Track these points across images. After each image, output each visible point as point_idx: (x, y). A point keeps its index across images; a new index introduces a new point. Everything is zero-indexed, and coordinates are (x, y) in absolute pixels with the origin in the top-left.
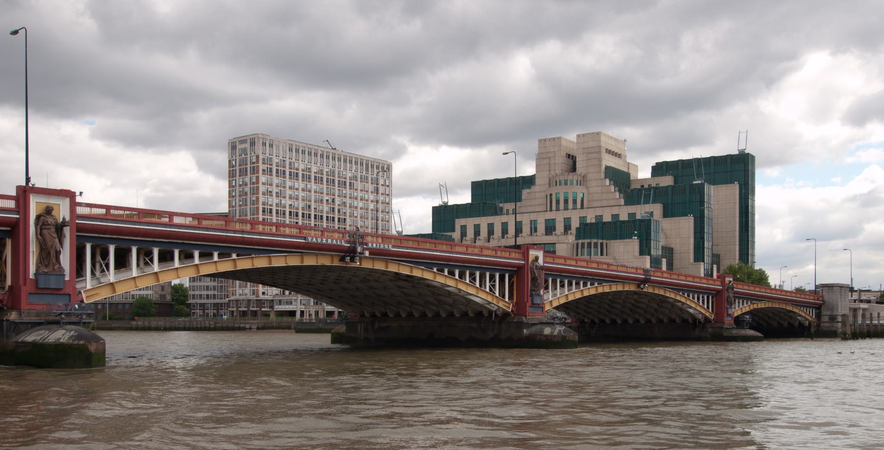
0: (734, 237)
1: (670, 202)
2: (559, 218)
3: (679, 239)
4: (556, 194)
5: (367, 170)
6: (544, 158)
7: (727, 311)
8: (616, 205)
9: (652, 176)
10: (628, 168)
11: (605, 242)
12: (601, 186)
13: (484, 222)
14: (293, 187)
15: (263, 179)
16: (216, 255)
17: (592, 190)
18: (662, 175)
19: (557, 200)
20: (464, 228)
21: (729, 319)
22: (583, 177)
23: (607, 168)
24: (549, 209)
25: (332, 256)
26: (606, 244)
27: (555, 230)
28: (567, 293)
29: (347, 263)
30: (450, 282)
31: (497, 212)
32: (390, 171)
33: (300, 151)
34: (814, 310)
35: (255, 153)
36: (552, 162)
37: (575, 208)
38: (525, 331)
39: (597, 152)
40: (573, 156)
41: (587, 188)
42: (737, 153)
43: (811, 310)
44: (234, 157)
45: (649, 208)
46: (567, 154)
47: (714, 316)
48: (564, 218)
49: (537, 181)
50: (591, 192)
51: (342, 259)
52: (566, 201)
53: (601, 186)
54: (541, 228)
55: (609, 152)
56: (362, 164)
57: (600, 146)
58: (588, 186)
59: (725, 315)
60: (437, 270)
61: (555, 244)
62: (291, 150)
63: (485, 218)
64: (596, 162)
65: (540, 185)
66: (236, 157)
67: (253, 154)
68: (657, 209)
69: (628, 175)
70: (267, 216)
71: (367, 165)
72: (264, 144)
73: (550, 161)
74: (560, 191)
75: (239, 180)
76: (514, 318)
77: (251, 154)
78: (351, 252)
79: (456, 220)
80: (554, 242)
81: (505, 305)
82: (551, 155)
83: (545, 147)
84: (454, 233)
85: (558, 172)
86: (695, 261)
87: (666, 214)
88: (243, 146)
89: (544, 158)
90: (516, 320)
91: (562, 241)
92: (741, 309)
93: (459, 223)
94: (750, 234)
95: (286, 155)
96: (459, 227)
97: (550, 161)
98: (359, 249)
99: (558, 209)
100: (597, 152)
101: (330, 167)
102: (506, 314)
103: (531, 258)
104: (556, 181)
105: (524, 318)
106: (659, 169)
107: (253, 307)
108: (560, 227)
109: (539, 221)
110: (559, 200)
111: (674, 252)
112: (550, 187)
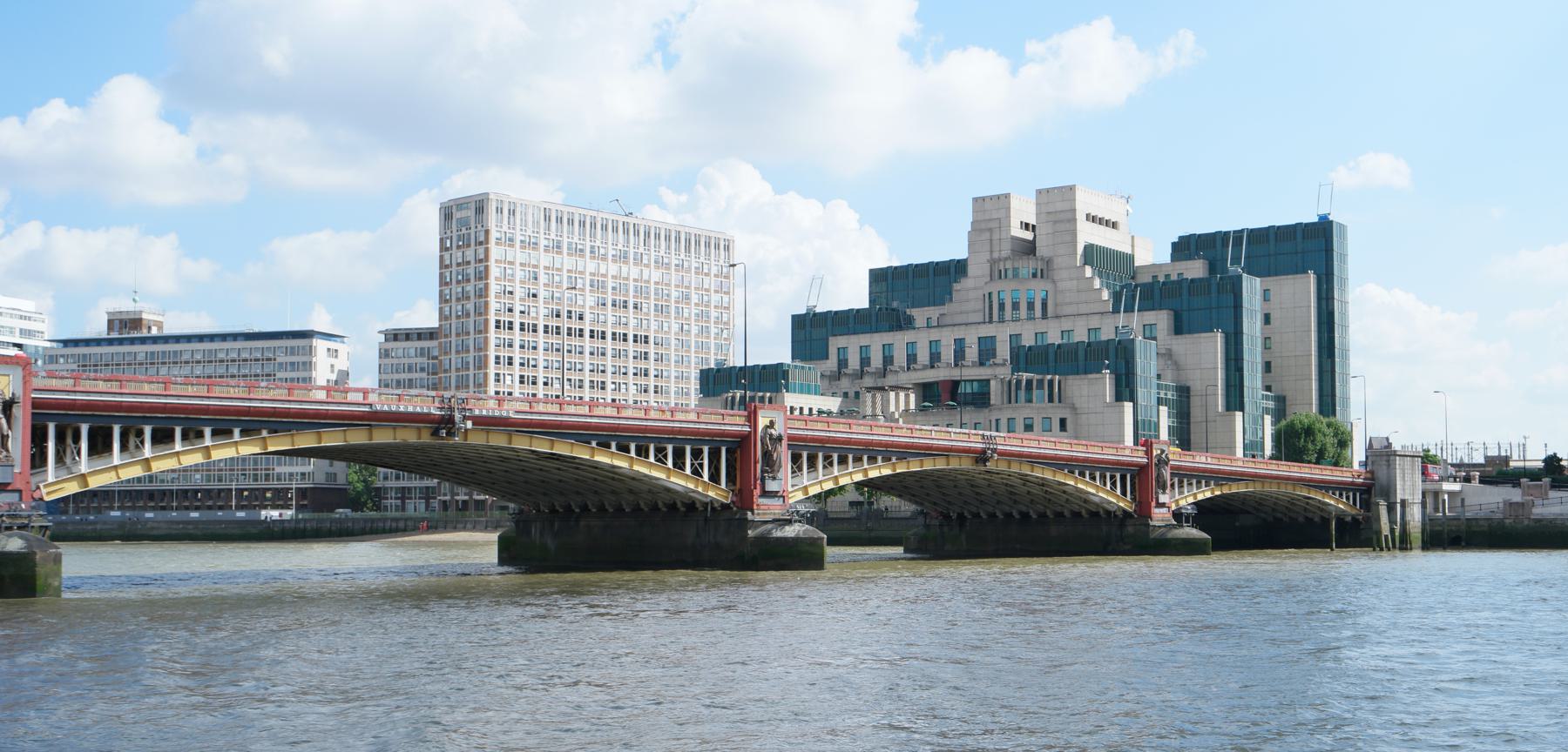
0: (1310, 365)
1: (1184, 308)
2: (1002, 336)
3: (1199, 371)
4: (999, 292)
5: (688, 249)
7: (1157, 499)
8: (1095, 311)
9: (1172, 261)
10: (1133, 246)
13: (876, 342)
16: (237, 432)
17: (1061, 285)
18: (1190, 258)
19: (1000, 304)
20: (842, 351)
21: (1164, 510)
23: (1089, 248)
24: (987, 320)
25: (419, 428)
26: (1059, 382)
27: (994, 356)
28: (836, 474)
29: (442, 438)
30: (621, 463)
31: (903, 323)
32: (731, 251)
33: (565, 220)
34: (1358, 495)
35: (482, 226)
36: (996, 236)
37: (1031, 318)
38: (749, 532)
42: (1316, 220)
43: (1351, 494)
45: (1150, 317)
46: (1021, 222)
47: (1136, 506)
48: (979, 338)
49: (971, 270)
51: (435, 433)
52: (1016, 306)
54: (972, 353)
55: (1093, 219)
56: (678, 239)
58: (1055, 278)
59: (1153, 504)
60: (597, 444)
62: (547, 218)
65: (975, 278)
66: (452, 232)
67: (479, 226)
68: (1161, 319)
69: (1131, 258)
70: (504, 334)
72: (499, 210)
73: (991, 236)
74: (1006, 290)
76: (736, 514)
77: (476, 227)
78: (445, 423)
81: (718, 494)
82: (993, 225)
83: (985, 211)
84: (828, 361)
87: (1178, 329)
88: (462, 214)
90: (737, 517)
92: (1195, 495)
93: (836, 343)
94: (1337, 360)
95: (539, 227)
96: (836, 351)
97: (991, 236)
98: (457, 416)
99: (1002, 320)
101: (620, 247)
102: (725, 507)
103: (762, 422)
104: (1000, 271)
105: (749, 513)
106: (1185, 247)
109: (968, 341)
110: (1004, 304)
111: (1192, 394)
112: (991, 279)
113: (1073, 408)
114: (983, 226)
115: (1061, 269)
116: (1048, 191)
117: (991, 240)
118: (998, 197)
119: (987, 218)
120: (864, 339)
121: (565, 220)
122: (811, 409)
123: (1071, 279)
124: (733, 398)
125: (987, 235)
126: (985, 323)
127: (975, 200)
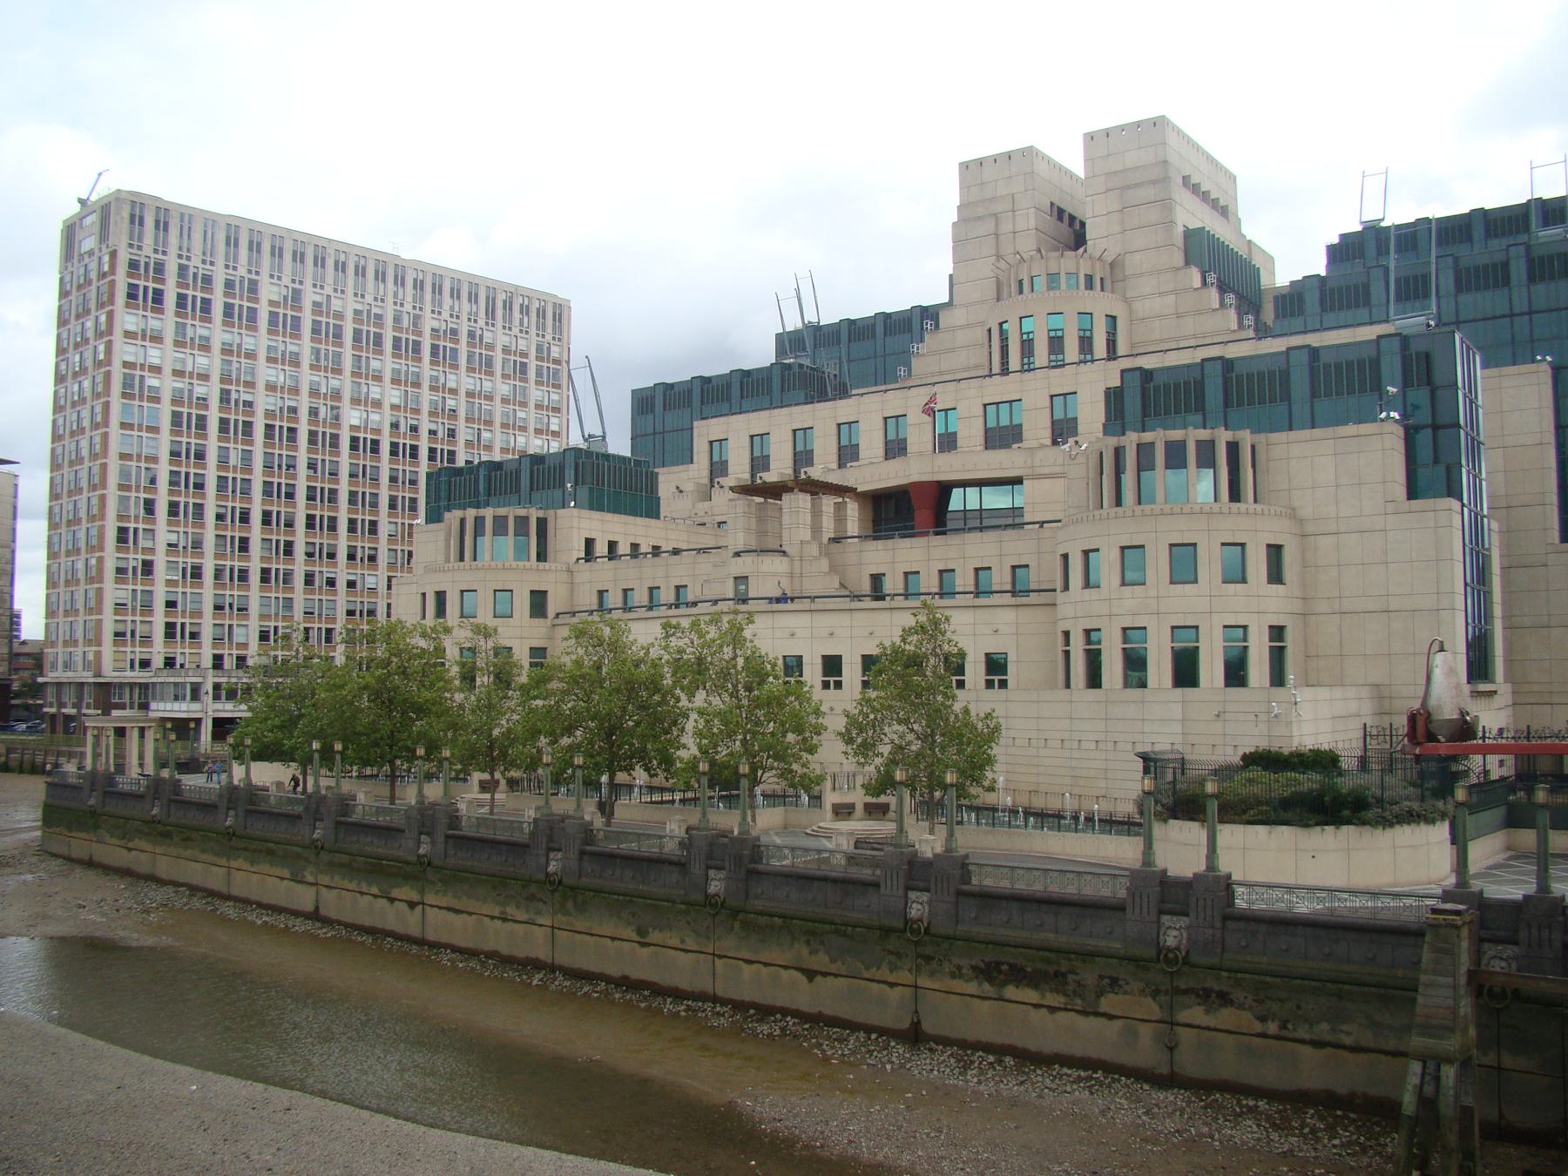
6: (979, 218)
11: (1246, 437)
12: (1174, 292)
14: (235, 348)
22: (1112, 265)
36: (1006, 227)
39: (1154, 182)
40: (1072, 218)
41: (1126, 300)
44: (70, 269)
46: (1052, 204)
50: (1141, 315)
53: (1174, 292)
58: (1128, 295)
63: (784, 411)
73: (997, 225)
75: (74, 326)
85: (1027, 245)
89: (979, 218)
91: (1046, 471)
97: (997, 225)
99: (1027, 368)
107: (88, 707)
108: (1037, 428)
113: (1293, 515)
120: (756, 421)
121: (266, 248)
123: (1161, 294)
125: (987, 227)
127: (965, 167)
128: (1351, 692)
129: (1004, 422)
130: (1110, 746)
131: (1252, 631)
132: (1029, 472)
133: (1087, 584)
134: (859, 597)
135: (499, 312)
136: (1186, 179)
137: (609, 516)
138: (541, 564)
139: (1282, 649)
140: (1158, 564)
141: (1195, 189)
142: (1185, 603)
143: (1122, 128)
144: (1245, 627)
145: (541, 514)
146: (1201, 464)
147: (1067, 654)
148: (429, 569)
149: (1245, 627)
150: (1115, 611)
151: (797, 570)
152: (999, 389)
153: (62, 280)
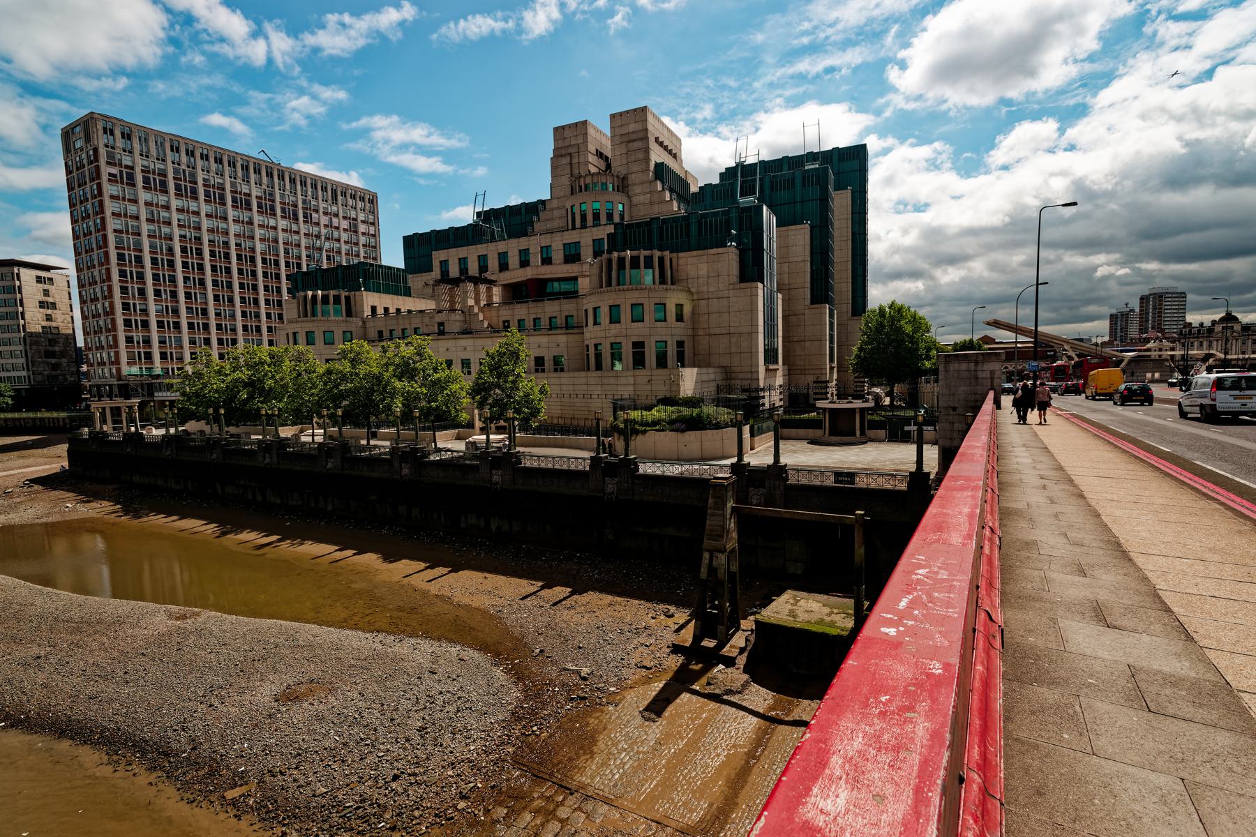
6: (562, 156)
12: (650, 192)
15: (109, 189)
17: (636, 200)
20: (444, 264)
22: (623, 179)
36: (575, 160)
39: (641, 139)
41: (629, 197)
44: (70, 157)
46: (597, 150)
54: (558, 256)
57: (647, 130)
61: (575, 279)
64: (641, 155)
67: (89, 146)
71: (334, 192)
79: (433, 253)
80: (574, 275)
86: (812, 303)
99: (584, 226)
100: (641, 139)
109: (554, 246)
110: (585, 215)
112: (572, 194)
114: (563, 152)
115: (635, 184)
116: (621, 114)
117: (571, 164)
118: (576, 124)
119: (567, 144)
120: (462, 252)
122: (386, 310)
123: (644, 194)
124: (305, 297)
126: (568, 230)
127: (556, 129)
128: (711, 370)
129: (573, 252)
130: (604, 397)
131: (669, 343)
132: (580, 274)
133: (595, 323)
134: (498, 332)
135: (340, 198)
136: (657, 139)
137: (383, 295)
138: (348, 319)
139: (683, 352)
140: (626, 315)
141: (661, 144)
142: (638, 331)
143: (628, 112)
144: (666, 342)
145: (347, 294)
146: (646, 267)
147: (588, 355)
148: (290, 322)
149: (666, 342)
150: (607, 335)
151: (468, 319)
152: (571, 237)
153: (66, 164)
